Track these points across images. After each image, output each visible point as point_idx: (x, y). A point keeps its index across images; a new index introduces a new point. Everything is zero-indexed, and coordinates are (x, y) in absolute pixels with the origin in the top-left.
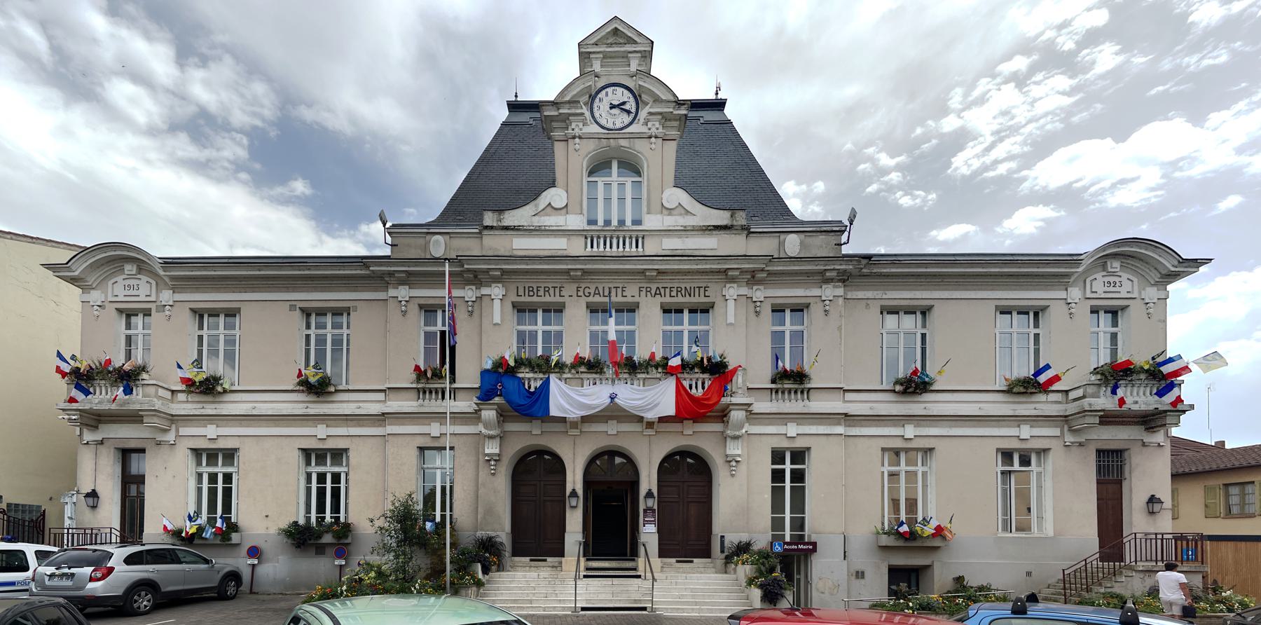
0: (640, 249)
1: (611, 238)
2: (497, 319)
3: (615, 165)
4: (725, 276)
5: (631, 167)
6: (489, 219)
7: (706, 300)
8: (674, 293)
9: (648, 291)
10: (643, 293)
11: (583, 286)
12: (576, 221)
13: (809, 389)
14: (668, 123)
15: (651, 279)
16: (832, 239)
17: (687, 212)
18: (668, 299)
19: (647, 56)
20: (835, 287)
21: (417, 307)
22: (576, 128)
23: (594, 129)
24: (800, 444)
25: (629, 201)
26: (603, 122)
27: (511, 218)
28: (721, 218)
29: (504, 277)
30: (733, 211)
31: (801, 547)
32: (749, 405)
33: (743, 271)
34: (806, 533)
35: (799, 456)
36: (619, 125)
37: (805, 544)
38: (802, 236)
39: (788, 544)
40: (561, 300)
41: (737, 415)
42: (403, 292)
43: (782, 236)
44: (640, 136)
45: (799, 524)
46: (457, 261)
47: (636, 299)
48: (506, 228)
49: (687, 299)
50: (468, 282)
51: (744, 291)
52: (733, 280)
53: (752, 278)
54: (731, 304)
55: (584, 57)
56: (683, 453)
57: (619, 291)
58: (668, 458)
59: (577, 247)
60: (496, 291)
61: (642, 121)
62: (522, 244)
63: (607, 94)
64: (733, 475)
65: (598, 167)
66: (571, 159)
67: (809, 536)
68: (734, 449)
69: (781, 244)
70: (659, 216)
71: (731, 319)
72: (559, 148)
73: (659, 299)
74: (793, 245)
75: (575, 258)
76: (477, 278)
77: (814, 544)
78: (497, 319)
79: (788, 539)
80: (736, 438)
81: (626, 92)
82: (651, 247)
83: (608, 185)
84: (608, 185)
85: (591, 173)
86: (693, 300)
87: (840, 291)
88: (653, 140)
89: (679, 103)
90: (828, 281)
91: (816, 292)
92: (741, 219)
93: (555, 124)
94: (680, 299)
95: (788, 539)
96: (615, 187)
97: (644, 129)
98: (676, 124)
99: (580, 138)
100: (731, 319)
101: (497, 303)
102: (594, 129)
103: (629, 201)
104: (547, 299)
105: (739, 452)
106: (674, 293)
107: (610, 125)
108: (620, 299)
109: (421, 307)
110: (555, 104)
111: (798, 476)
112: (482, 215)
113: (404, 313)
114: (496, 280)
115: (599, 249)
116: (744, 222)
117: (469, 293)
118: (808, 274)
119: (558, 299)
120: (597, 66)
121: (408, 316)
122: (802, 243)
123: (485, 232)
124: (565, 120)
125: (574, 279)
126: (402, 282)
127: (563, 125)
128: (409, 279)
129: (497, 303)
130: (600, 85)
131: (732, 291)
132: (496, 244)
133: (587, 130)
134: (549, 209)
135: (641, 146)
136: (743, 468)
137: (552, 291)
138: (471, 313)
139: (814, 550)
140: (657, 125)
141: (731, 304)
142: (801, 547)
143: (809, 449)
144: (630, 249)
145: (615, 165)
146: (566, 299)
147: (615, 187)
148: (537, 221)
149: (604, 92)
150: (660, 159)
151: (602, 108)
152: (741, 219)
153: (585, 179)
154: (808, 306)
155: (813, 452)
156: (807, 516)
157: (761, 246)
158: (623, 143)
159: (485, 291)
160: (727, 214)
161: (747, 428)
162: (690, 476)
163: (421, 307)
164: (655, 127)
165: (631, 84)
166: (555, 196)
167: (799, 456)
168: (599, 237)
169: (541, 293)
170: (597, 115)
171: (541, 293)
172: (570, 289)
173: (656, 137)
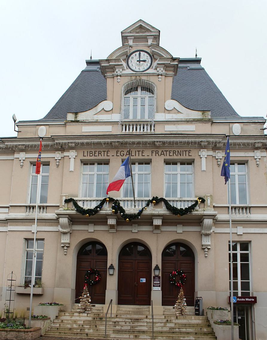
0: (152, 131)
1: (137, 125)
2: (72, 169)
3: (139, 89)
4: (200, 146)
5: (148, 89)
6: (70, 117)
7: (190, 158)
8: (171, 154)
9: (157, 153)
12: (116, 117)
13: (250, 207)
14: (168, 69)
15: (159, 147)
16: (259, 126)
17: (179, 112)
18: (168, 157)
19: (157, 37)
20: (261, 152)
21: (29, 163)
22: (118, 71)
23: (129, 71)
24: (244, 239)
25: (147, 107)
26: (134, 68)
27: (82, 117)
28: (197, 115)
29: (76, 147)
30: (204, 111)
31: (247, 299)
32: (214, 216)
33: (209, 143)
34: (251, 291)
35: (245, 246)
36: (141, 70)
37: (250, 298)
38: (242, 124)
39: (240, 298)
40: (108, 158)
41: (207, 222)
42: (22, 156)
43: (231, 125)
44: (153, 75)
45: (246, 286)
46: (52, 139)
47: (150, 157)
48: (78, 121)
49: (179, 157)
50: (57, 150)
51: (211, 153)
52: (205, 147)
53: (215, 147)
54: (204, 160)
55: (125, 38)
56: (178, 244)
57: (140, 153)
58: (168, 247)
59: (117, 130)
60: (72, 154)
61: (154, 67)
62: (87, 130)
63: (136, 55)
64: (206, 257)
65: (131, 89)
66: (115, 86)
67: (252, 293)
68: (206, 241)
69: (231, 129)
70: (163, 114)
71: (204, 168)
72: (109, 81)
73: (163, 157)
74: (237, 129)
75: (115, 136)
76: (62, 148)
77: (255, 298)
78: (72, 169)
79: (240, 295)
80: (207, 235)
81: (146, 54)
82: (159, 130)
83: (135, 99)
84: (135, 99)
85: (128, 92)
86: (182, 157)
88: (160, 76)
89: (174, 59)
90: (257, 148)
91: (251, 154)
92: (209, 115)
93: (107, 70)
94: (175, 157)
95: (240, 295)
96: (139, 100)
97: (155, 71)
98: (172, 69)
99: (120, 76)
100: (204, 168)
101: (72, 160)
102: (129, 71)
103: (147, 107)
104: (100, 157)
105: (209, 243)
106: (171, 154)
107: (137, 70)
108: (141, 157)
109: (31, 163)
110: (108, 61)
111: (245, 258)
112: (66, 115)
113: (22, 166)
114: (72, 148)
115: (130, 131)
116: (210, 117)
117: (58, 155)
119: (106, 157)
120: (131, 42)
121: (24, 167)
122: (242, 129)
123: (68, 124)
124: (113, 68)
125: (116, 147)
126: (22, 151)
127: (112, 70)
128: (26, 149)
129: (72, 160)
130: (132, 51)
131: (204, 153)
132: (73, 130)
133: (124, 72)
134: (103, 111)
136: (211, 252)
137: (102, 153)
138: (58, 166)
139: (255, 301)
140: (162, 69)
141: (204, 160)
142: (247, 299)
143: (250, 242)
144: (147, 130)
145: (139, 89)
146: (110, 157)
147: (139, 100)
148: (96, 118)
149: (134, 54)
150: (164, 85)
151: (133, 61)
152: (209, 115)
153: (123, 96)
154: (247, 162)
155: (252, 243)
156: (250, 281)
157: (220, 130)
158: (144, 78)
159: (66, 154)
160: (200, 113)
161: (213, 229)
162: (182, 256)
163: (31, 163)
164: (161, 70)
165: (149, 51)
166: (106, 105)
167: (245, 246)
168: (129, 125)
169: (97, 154)
170: (130, 65)
171: (97, 154)
172: (112, 152)
173: (161, 75)
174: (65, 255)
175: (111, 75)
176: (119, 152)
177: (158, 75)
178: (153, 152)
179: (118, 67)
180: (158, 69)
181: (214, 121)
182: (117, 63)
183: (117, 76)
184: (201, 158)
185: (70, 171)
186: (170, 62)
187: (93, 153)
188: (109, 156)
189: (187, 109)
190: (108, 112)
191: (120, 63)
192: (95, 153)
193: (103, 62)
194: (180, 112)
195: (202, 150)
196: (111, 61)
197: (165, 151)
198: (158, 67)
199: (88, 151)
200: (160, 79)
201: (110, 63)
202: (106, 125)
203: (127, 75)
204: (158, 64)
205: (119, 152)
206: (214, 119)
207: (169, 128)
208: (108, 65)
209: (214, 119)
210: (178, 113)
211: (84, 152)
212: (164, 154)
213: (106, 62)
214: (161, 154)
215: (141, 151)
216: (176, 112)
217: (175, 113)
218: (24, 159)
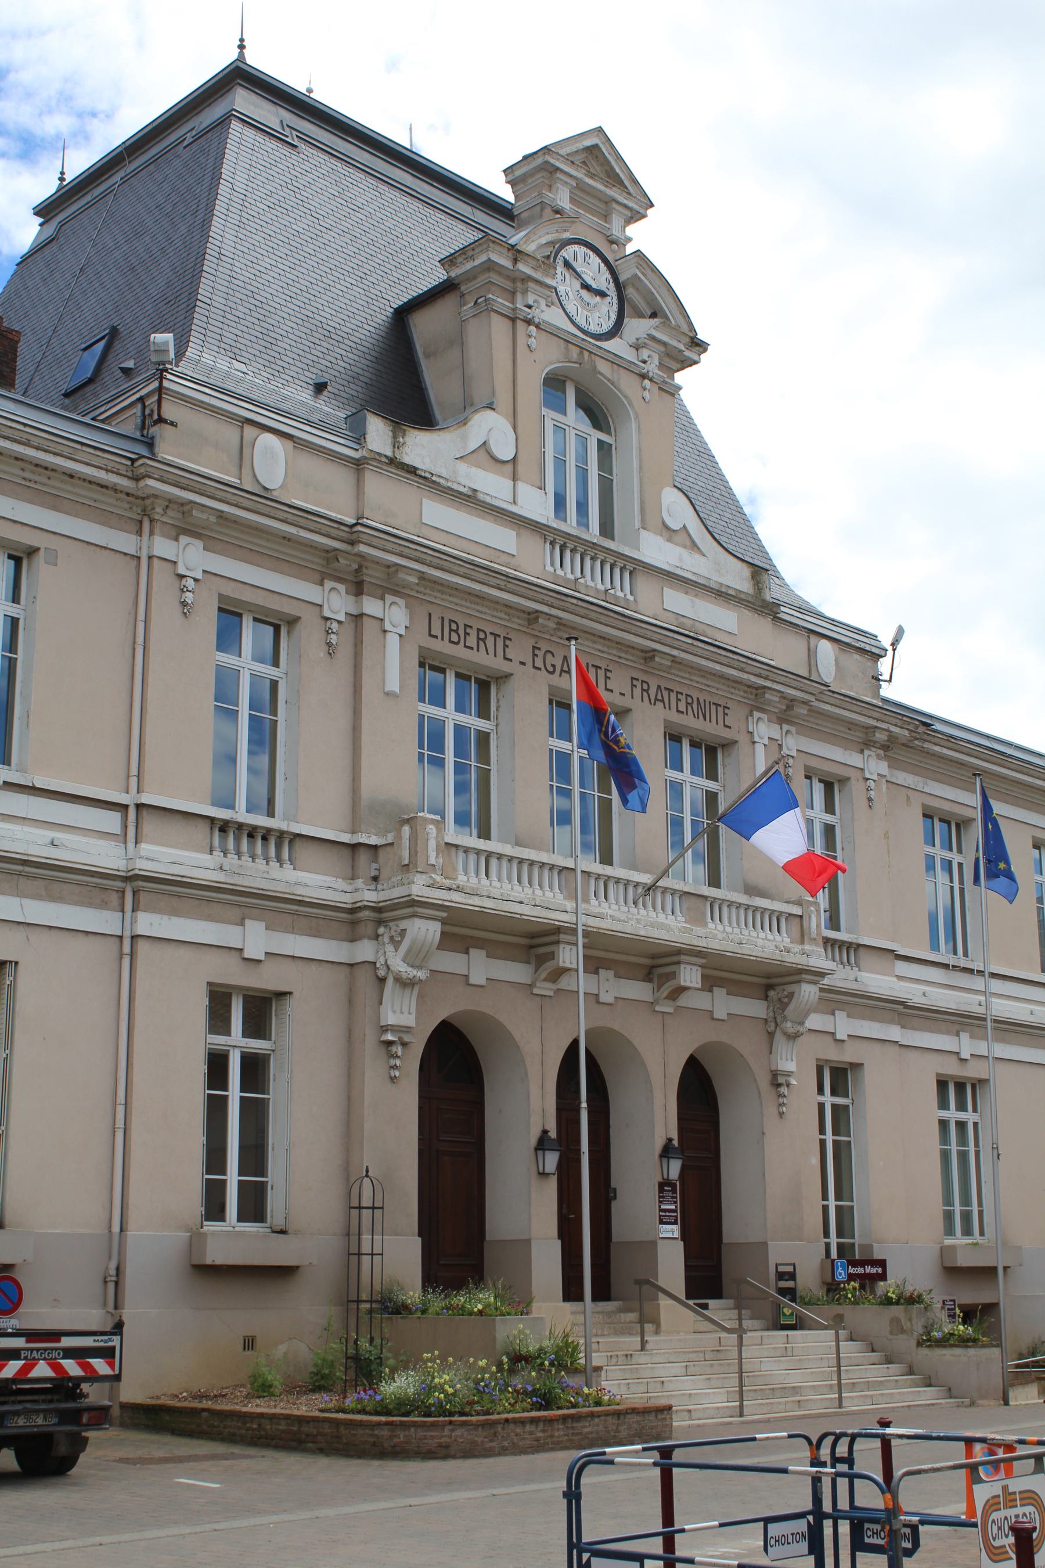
4: (756, 698)
10: (637, 691)
11: (544, 646)
17: (694, 546)
18: (674, 717)
40: (505, 667)
42: (193, 557)
44: (625, 366)
60: (396, 615)
62: (439, 517)
78: (393, 684)
87: (883, 767)
91: (855, 759)
97: (629, 355)
118: (851, 725)
134: (482, 453)
135: (628, 384)
158: (603, 367)
171: (472, 641)
174: (393, 1079)
175: (508, 308)
176: (540, 654)
177: (643, 376)
178: (635, 682)
179: (538, 288)
180: (645, 354)
181: (781, 615)
182: (538, 275)
183: (529, 322)
184: (754, 743)
185: (387, 694)
186: (682, 347)
187: (461, 632)
188: (511, 660)
189: (715, 544)
190: (499, 465)
191: (552, 283)
192: (466, 634)
193: (498, 248)
194: (698, 548)
195: (757, 714)
196: (526, 258)
197: (666, 689)
198: (645, 346)
199: (443, 618)
200: (647, 395)
201: (521, 267)
202: (495, 522)
203: (553, 332)
204: (653, 338)
205: (540, 654)
206: (782, 609)
207: (678, 603)
208: (505, 262)
209: (782, 609)
210: (693, 549)
211: (430, 615)
212: (663, 701)
213: (505, 251)
214: (656, 699)
215: (604, 667)
216: (688, 543)
217: (685, 547)
218: (199, 575)
